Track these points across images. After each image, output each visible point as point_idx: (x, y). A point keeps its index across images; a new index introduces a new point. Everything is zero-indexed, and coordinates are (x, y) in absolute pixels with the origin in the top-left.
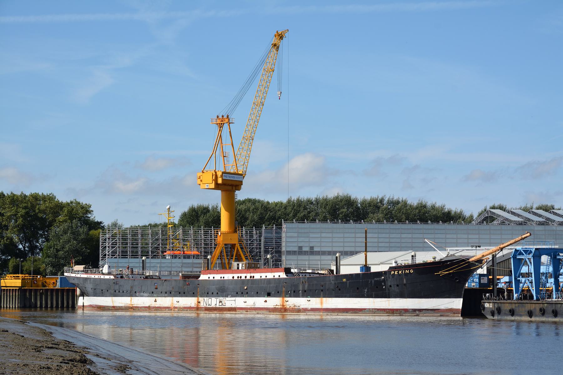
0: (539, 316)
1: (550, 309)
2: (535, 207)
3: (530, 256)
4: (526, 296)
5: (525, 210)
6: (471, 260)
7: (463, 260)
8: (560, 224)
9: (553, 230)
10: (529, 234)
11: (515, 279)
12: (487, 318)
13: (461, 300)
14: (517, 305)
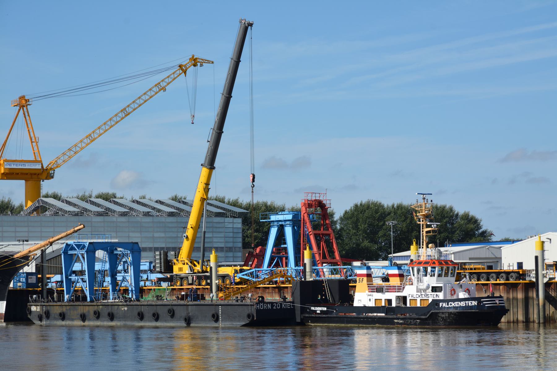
0: (93, 320)
1: (105, 312)
2: (94, 195)
3: (83, 252)
4: (79, 297)
5: (83, 199)
6: (16, 256)
7: (6, 257)
8: (121, 215)
9: (114, 222)
10: (82, 226)
11: (66, 277)
12: (34, 324)
13: (5, 302)
14: (68, 308)
